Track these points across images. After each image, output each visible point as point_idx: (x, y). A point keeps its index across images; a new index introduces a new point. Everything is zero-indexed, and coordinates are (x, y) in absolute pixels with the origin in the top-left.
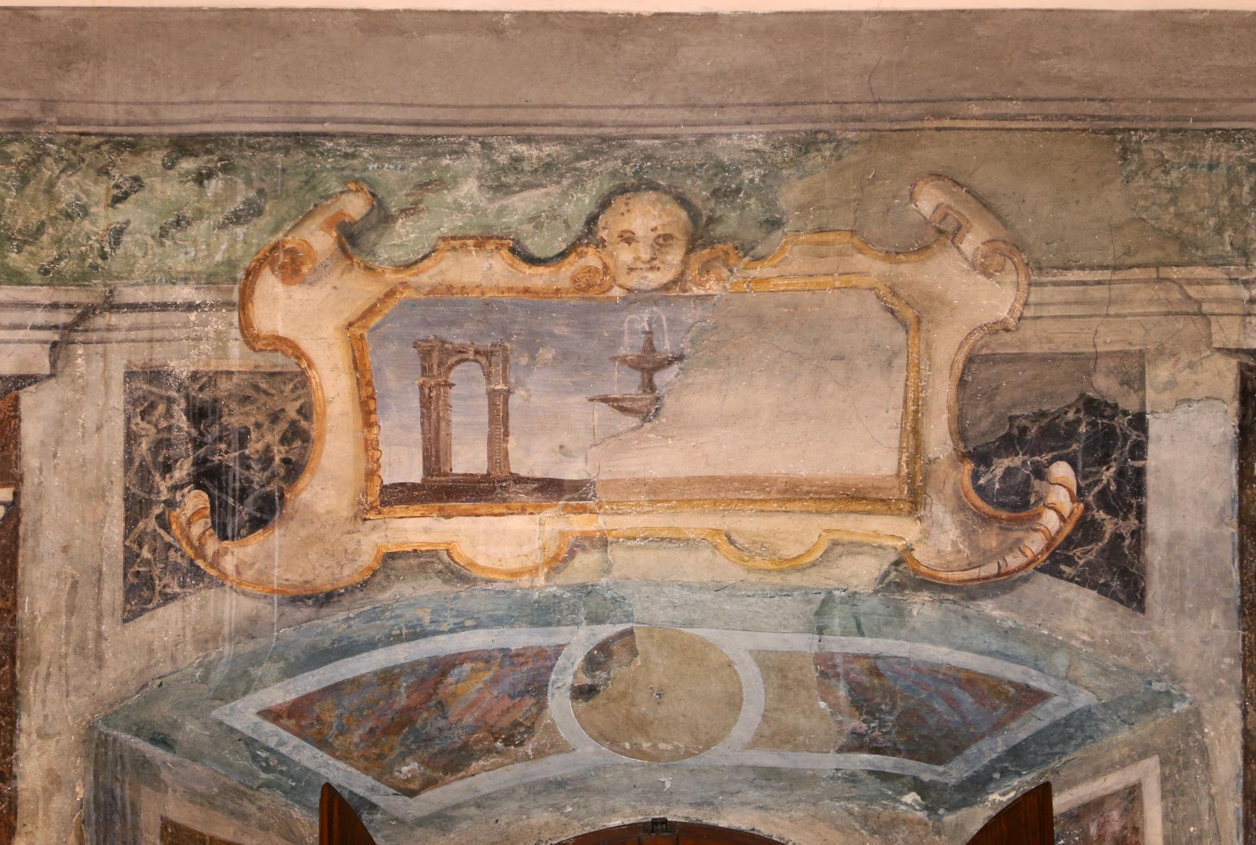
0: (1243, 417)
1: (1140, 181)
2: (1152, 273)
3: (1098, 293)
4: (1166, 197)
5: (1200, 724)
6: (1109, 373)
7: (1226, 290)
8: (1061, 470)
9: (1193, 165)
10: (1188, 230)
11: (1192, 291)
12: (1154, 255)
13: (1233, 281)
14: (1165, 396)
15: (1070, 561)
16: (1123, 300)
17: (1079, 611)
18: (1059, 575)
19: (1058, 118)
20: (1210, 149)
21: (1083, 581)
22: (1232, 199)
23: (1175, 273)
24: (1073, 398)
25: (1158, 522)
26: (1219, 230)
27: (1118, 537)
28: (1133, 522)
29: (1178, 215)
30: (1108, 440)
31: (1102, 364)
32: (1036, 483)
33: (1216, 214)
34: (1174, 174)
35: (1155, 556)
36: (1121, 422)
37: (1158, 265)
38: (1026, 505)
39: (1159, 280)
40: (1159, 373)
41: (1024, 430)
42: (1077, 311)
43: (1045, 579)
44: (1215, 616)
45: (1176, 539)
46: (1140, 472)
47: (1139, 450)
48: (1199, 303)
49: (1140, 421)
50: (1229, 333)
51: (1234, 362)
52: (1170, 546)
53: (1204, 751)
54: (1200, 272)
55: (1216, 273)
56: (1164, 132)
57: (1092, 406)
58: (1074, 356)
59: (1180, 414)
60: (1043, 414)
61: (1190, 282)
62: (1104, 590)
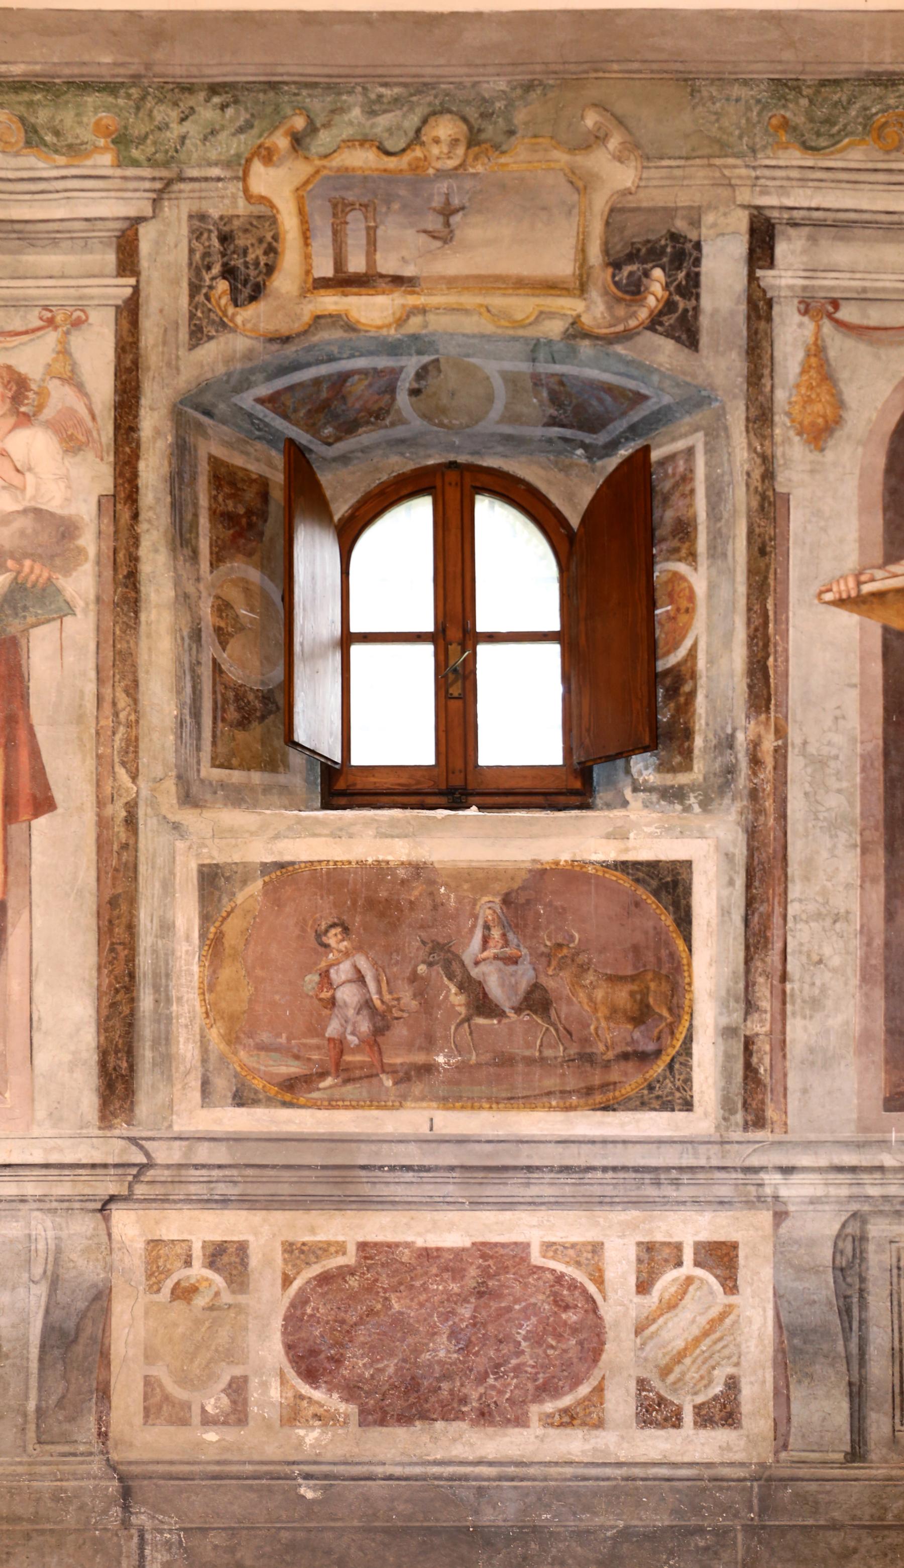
0: (751, 243)
1: (700, 109)
2: (705, 161)
3: (678, 172)
4: (713, 118)
5: (724, 414)
6: (683, 218)
7: (743, 172)
8: (658, 273)
9: (728, 100)
10: (725, 137)
11: (727, 172)
12: (706, 151)
13: (747, 166)
14: (712, 232)
15: (661, 324)
16: (690, 177)
17: (664, 352)
18: (655, 331)
19: (658, 72)
20: (737, 91)
21: (668, 335)
22: (748, 120)
23: (717, 161)
24: (664, 232)
25: (706, 303)
26: (740, 137)
27: (686, 311)
28: (694, 302)
29: (720, 128)
30: (681, 256)
31: (679, 213)
32: (644, 280)
33: (739, 128)
34: (718, 105)
35: (704, 321)
36: (689, 246)
37: (709, 157)
38: (638, 292)
39: (710, 165)
40: (709, 218)
41: (639, 250)
42: (667, 182)
43: (648, 334)
44: (734, 355)
45: (715, 311)
46: (698, 275)
47: (697, 262)
48: (730, 179)
49: (698, 246)
50: (745, 196)
51: (747, 213)
52: (712, 315)
53: (726, 428)
54: (731, 161)
55: (738, 162)
56: (713, 80)
57: (674, 237)
58: (665, 209)
59: (719, 242)
60: (648, 241)
61: (726, 167)
62: (678, 340)
